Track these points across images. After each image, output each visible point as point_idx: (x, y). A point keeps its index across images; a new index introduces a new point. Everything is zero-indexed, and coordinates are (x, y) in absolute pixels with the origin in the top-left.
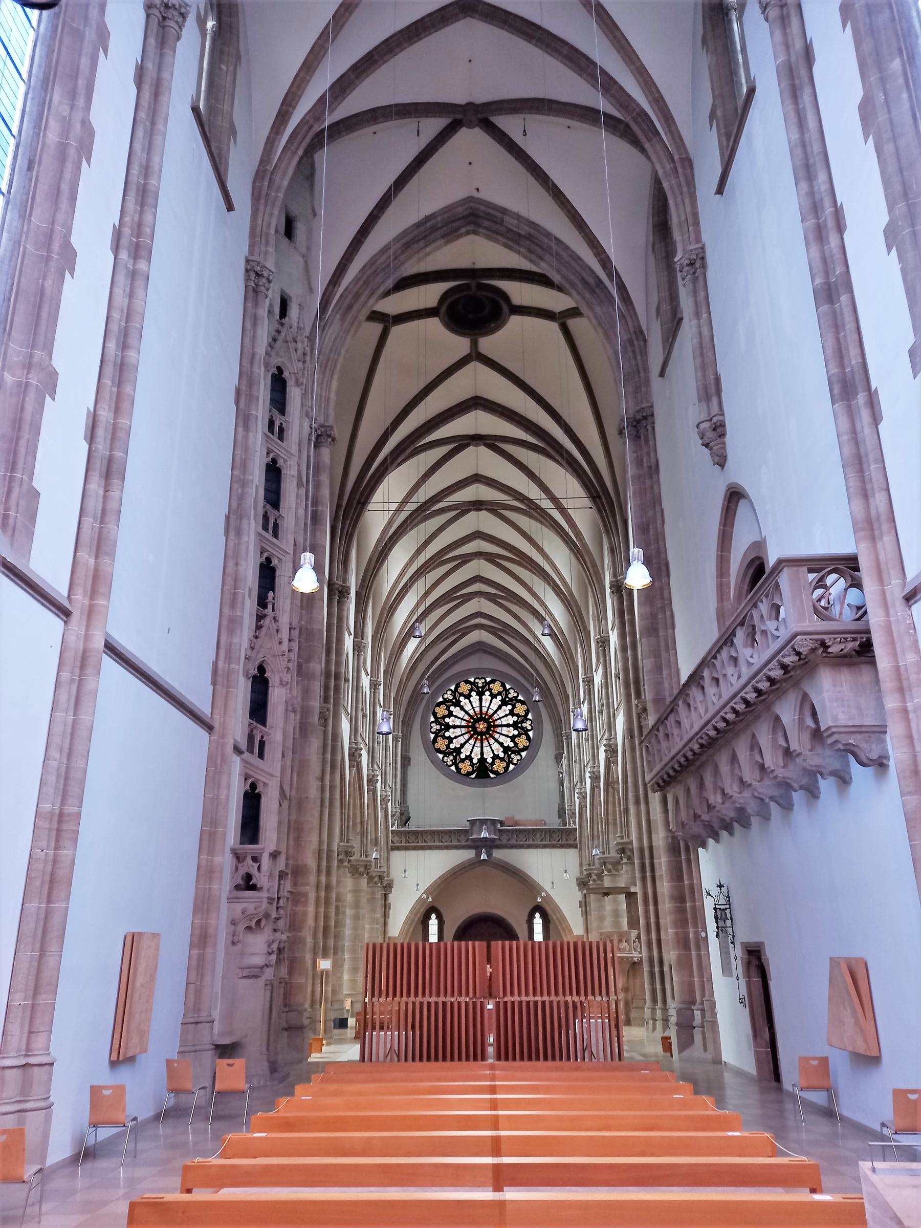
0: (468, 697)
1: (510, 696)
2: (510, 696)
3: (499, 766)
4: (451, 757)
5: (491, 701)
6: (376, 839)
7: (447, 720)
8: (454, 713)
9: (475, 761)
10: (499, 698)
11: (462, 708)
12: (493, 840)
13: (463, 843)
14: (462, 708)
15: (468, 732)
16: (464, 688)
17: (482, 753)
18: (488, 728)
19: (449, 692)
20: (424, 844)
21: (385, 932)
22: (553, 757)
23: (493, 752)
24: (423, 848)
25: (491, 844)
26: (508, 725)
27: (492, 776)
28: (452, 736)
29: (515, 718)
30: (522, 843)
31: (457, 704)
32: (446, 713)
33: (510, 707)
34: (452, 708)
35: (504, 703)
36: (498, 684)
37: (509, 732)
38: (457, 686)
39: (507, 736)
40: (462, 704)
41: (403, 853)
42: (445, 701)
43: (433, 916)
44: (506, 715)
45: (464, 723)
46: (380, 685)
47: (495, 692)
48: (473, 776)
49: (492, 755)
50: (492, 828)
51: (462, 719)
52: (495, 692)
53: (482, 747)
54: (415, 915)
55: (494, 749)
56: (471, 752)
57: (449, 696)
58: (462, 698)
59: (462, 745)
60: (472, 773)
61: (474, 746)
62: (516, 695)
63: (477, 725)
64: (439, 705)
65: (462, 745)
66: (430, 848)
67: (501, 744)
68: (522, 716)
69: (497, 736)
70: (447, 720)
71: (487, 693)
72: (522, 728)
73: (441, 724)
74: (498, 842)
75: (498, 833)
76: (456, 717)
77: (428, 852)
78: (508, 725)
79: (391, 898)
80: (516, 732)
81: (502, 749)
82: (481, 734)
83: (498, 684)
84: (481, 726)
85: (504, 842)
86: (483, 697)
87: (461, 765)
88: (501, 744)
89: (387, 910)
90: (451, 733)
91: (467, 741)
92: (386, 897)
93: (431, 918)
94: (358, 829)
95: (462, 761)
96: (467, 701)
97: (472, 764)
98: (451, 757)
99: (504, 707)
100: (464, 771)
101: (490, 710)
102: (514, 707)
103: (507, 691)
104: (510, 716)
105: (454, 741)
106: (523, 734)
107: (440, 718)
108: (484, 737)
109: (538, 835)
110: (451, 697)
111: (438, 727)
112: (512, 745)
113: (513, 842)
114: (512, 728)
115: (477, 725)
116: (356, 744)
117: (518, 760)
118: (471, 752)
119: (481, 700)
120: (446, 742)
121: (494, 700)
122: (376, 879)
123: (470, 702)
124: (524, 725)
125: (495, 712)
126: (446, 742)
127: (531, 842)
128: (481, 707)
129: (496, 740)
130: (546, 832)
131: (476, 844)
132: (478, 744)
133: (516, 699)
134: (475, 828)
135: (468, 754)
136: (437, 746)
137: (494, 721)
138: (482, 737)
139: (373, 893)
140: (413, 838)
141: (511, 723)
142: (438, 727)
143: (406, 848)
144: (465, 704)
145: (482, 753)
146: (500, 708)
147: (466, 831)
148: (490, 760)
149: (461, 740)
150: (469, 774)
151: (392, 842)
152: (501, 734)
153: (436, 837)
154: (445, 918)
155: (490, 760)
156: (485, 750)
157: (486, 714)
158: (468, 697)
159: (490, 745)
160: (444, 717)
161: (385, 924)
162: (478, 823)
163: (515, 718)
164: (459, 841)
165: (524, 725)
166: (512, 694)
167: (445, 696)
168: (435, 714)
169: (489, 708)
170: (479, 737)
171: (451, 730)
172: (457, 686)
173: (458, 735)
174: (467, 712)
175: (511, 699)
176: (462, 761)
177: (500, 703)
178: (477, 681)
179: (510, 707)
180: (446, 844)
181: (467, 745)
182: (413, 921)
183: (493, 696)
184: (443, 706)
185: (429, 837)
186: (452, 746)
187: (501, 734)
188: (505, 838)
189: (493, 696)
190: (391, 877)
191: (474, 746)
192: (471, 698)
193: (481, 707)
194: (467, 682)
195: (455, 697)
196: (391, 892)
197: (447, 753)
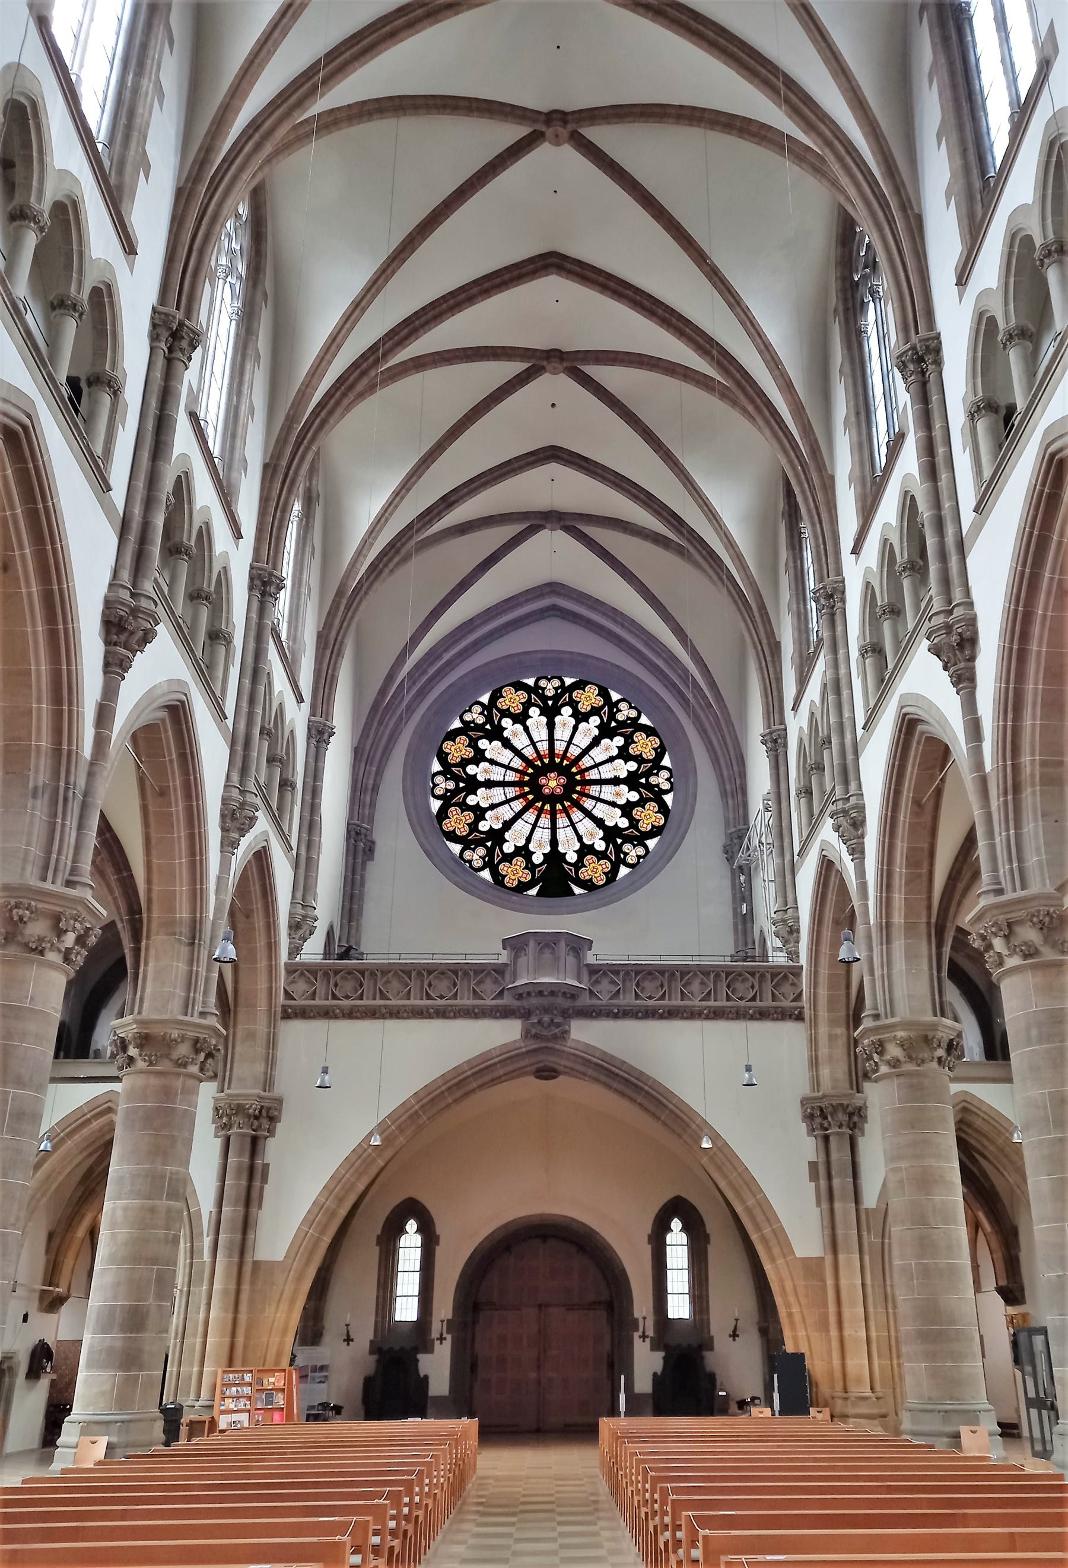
0: (521, 718)
1: (620, 717)
2: (620, 717)
3: (595, 870)
4: (482, 851)
5: (575, 729)
6: (195, 927)
7: (471, 769)
8: (488, 755)
9: (537, 859)
10: (595, 720)
11: (507, 744)
12: (572, 994)
13: (489, 1002)
14: (507, 744)
15: (523, 796)
16: (512, 700)
17: (554, 842)
18: (569, 788)
19: (477, 709)
20: (379, 1002)
21: (243, 1247)
22: (719, 849)
23: (580, 838)
24: (372, 1014)
25: (567, 1003)
26: (615, 781)
27: (577, 890)
28: (484, 804)
29: (632, 766)
30: (651, 1002)
31: (496, 734)
32: (470, 753)
33: (619, 741)
34: (483, 744)
35: (606, 731)
36: (592, 691)
37: (618, 794)
38: (496, 695)
39: (613, 804)
40: (506, 734)
41: (319, 1026)
42: (467, 728)
43: (412, 1226)
44: (611, 759)
45: (511, 776)
46: (280, 588)
47: (584, 707)
48: (533, 892)
49: (577, 846)
50: (571, 960)
51: (507, 767)
52: (584, 707)
53: (554, 829)
54: (340, 1200)
55: (581, 831)
56: (529, 839)
57: (476, 716)
58: (506, 722)
59: (508, 825)
61: (535, 826)
62: (633, 714)
63: (543, 781)
64: (452, 736)
65: (508, 825)
66: (395, 1014)
67: (599, 823)
68: (648, 761)
69: (588, 804)
70: (471, 769)
71: (567, 711)
72: (649, 786)
73: (456, 779)
74: (585, 1000)
75: (585, 976)
76: (492, 762)
77: (391, 1024)
78: (615, 781)
79: (273, 1150)
80: (634, 796)
81: (601, 834)
82: (553, 799)
83: (592, 691)
84: (552, 783)
85: (604, 1000)
86: (557, 719)
88: (599, 823)
89: (257, 1184)
90: (480, 798)
91: (518, 816)
92: (255, 1145)
93: (402, 1231)
94: (40, 773)
95: (508, 858)
96: (519, 727)
98: (482, 851)
99: (605, 742)
100: (511, 881)
101: (572, 748)
102: (629, 740)
103: (613, 706)
104: (621, 762)
105: (488, 815)
106: (650, 800)
107: (456, 765)
108: (559, 807)
109: (695, 986)
110: (480, 720)
111: (451, 785)
112: (624, 823)
113: (628, 1000)
114: (624, 788)
115: (543, 781)
116: (242, 792)
117: (639, 857)
118: (529, 839)
119: (551, 726)
120: (470, 817)
121: (583, 726)
122: (183, 1050)
123: (526, 729)
124: (653, 780)
125: (586, 752)
126: (470, 817)
127: (677, 1002)
128: (551, 740)
129: (588, 814)
130: (717, 976)
131: (525, 1003)
132: (545, 821)
133: (634, 724)
134: (522, 960)
135: (521, 843)
136: (448, 825)
137: (582, 772)
138: (553, 807)
139: (167, 1093)
140: (348, 986)
141: (623, 775)
142: (451, 785)
143: (327, 1014)
144: (515, 734)
145: (554, 842)
146: (595, 742)
147: (499, 970)
148: (572, 857)
149: (506, 813)
150: (522, 887)
151: (288, 995)
152: (598, 799)
153: (414, 984)
154: (440, 1229)
155: (572, 857)
156: (561, 835)
157: (564, 756)
158: (521, 718)
159: (573, 824)
160: (464, 763)
161: (246, 1225)
162: (532, 944)
163: (632, 766)
164: (476, 995)
165: (653, 780)
166: (625, 712)
167: (468, 717)
168: (442, 757)
169: (570, 742)
170: (547, 807)
171: (481, 791)
172: (496, 695)
173: (495, 801)
174: (518, 753)
175: (622, 724)
176: (508, 858)
177: (596, 732)
178: (543, 683)
179: (619, 741)
180: (440, 1002)
181: (519, 823)
182: (333, 1214)
183: (580, 717)
184: (463, 739)
185: (395, 985)
186: (483, 826)
187: (598, 799)
188: (605, 989)
189: (580, 717)
190: (279, 1090)
191: (535, 826)
192: (529, 722)
193: (551, 740)
194: (519, 686)
195: (489, 719)
196: (271, 1132)
197: (473, 842)
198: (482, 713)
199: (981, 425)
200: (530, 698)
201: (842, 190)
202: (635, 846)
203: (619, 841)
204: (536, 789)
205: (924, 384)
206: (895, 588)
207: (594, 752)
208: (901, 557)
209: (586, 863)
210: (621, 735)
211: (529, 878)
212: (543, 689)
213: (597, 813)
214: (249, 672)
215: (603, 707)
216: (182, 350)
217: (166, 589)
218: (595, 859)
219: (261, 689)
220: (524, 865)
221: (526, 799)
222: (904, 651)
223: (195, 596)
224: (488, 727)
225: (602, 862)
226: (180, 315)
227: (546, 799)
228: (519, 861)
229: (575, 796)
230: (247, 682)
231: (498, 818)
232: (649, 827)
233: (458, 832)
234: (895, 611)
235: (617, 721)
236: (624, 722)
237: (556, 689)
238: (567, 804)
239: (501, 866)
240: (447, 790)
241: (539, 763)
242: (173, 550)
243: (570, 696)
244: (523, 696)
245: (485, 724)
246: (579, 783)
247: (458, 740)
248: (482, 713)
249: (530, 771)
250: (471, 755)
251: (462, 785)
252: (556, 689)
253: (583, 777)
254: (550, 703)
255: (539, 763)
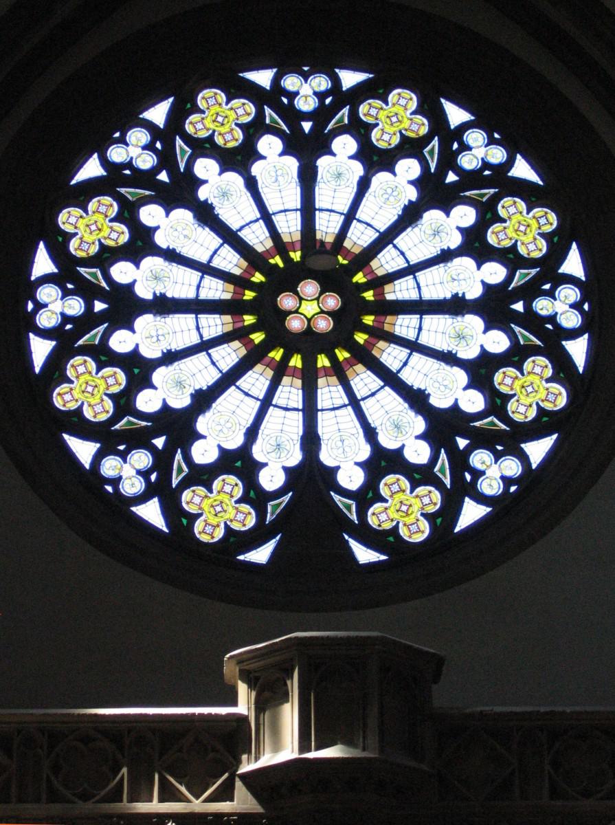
2: (468, 162)
8: (161, 240)
9: (272, 479)
11: (206, 215)
14: (206, 215)
15: (239, 334)
17: (311, 441)
18: (346, 319)
26: (455, 306)
28: (151, 352)
29: (495, 273)
32: (121, 235)
40: (203, 193)
44: (445, 256)
45: (215, 290)
47: (385, 137)
52: (385, 137)
53: (310, 411)
58: (205, 168)
59: (204, 399)
60: (254, 538)
65: (204, 399)
67: (417, 399)
68: (531, 263)
69: (391, 356)
70: (122, 272)
71: (345, 145)
72: (532, 321)
78: (455, 306)
82: (309, 343)
87: (191, 499)
88: (417, 399)
96: (234, 180)
97: (255, 497)
99: (433, 217)
105: (159, 376)
106: (535, 351)
107: (88, 262)
108: (323, 361)
110: (146, 162)
111: (75, 307)
114: (474, 323)
115: (286, 302)
119: (308, 178)
124: (543, 306)
126: (117, 378)
129: (391, 379)
133: (500, 179)
137: (379, 283)
138: (309, 362)
141: (474, 292)
142: (75, 307)
145: (311, 441)
146: (410, 216)
148: (351, 478)
155: (351, 478)
159: (354, 403)
165: (543, 306)
170: (296, 361)
173: (178, 344)
175: (472, 179)
177: (412, 194)
179: (465, 215)
191: (266, 403)
198: (149, 147)
200: (260, 115)
202: (498, 456)
203: (462, 443)
204: (272, 320)
207: (405, 240)
209: (384, 491)
210: (470, 202)
211: (251, 522)
212: (292, 95)
213: (411, 377)
215: (426, 140)
218: (405, 483)
220: (239, 492)
221: (248, 343)
224: (163, 176)
225: (422, 490)
227: (292, 343)
228: (229, 485)
229: (361, 338)
231: (180, 384)
232: (532, 414)
233: (88, 414)
235: (459, 170)
236: (476, 174)
237: (321, 96)
238: (342, 355)
239: (186, 495)
240: (66, 319)
241: (278, 261)
243: (354, 114)
244: (245, 110)
245: (155, 170)
246: (369, 308)
247: (92, 205)
248: (149, 147)
249: (258, 278)
250: (124, 238)
251: (99, 306)
252: (321, 96)
253: (380, 294)
254: (307, 126)
255: (278, 261)
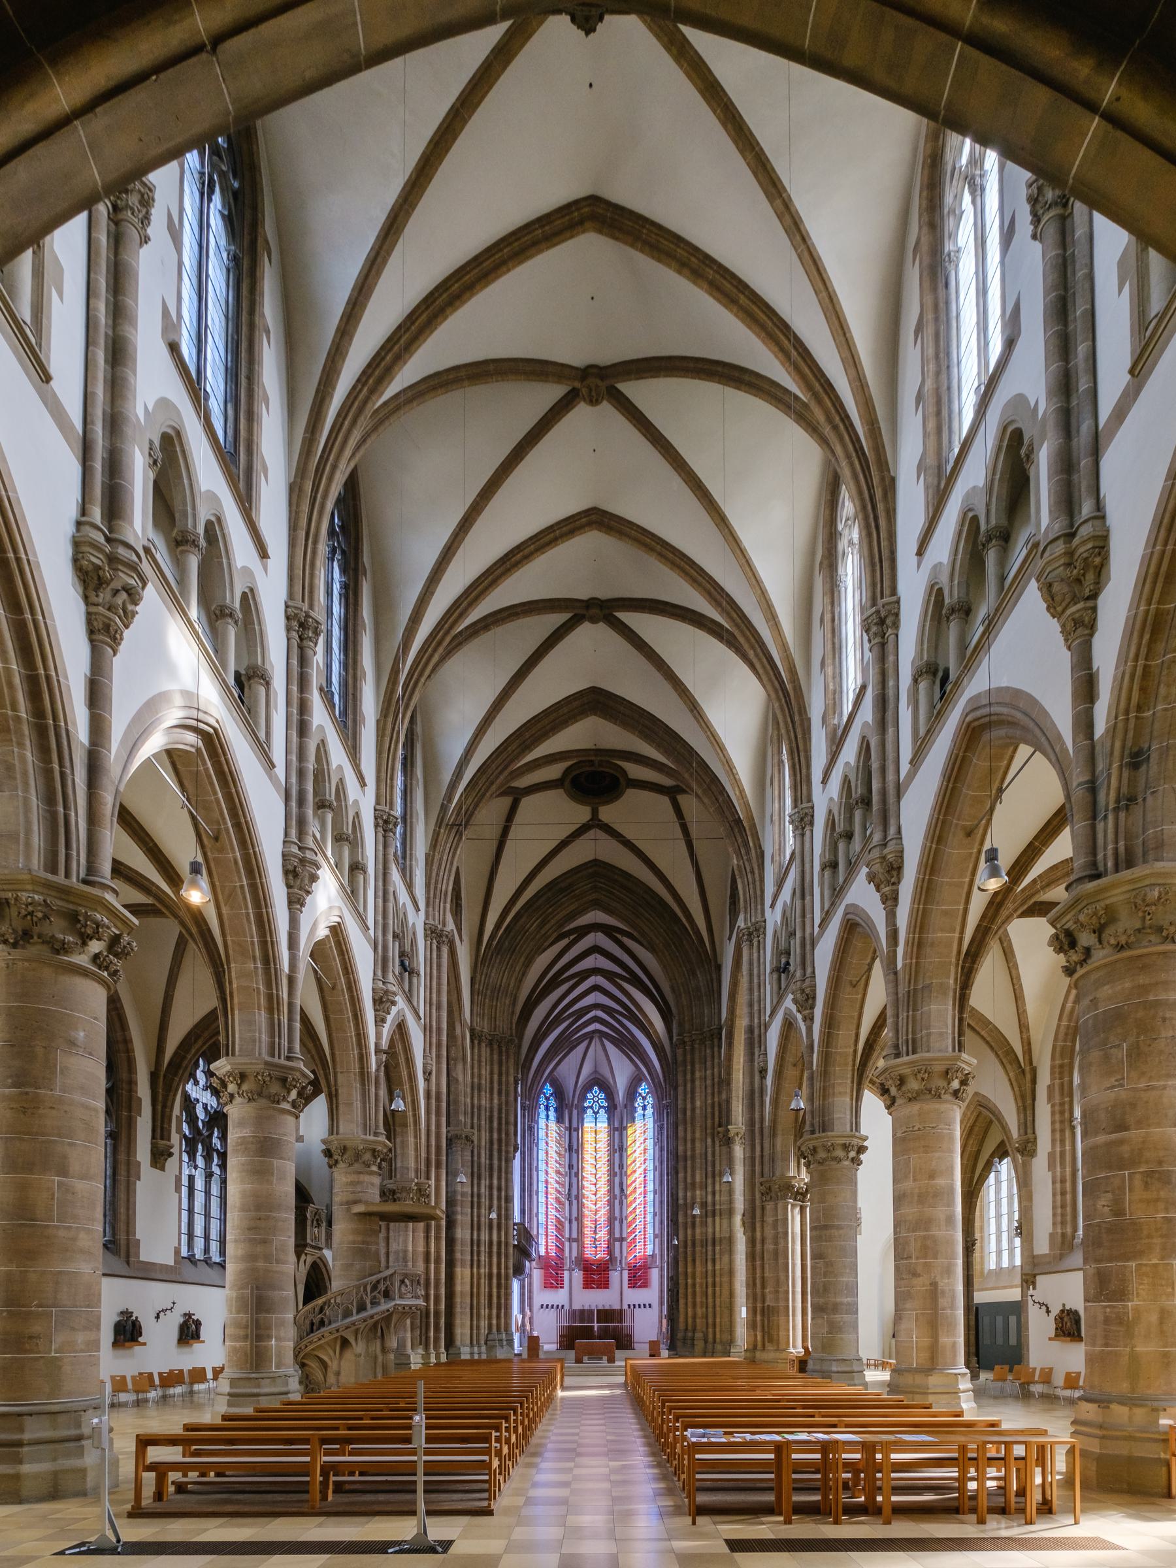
199: (923, 685)
201: (833, 452)
205: (883, 645)
206: (850, 819)
208: (858, 791)
214: (380, 894)
216: (310, 639)
217: (318, 836)
219: (391, 905)
222: (852, 867)
223: (339, 839)
226: (305, 607)
230: (380, 901)
234: (849, 836)
242: (321, 805)
